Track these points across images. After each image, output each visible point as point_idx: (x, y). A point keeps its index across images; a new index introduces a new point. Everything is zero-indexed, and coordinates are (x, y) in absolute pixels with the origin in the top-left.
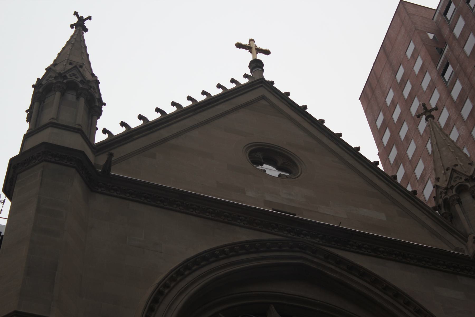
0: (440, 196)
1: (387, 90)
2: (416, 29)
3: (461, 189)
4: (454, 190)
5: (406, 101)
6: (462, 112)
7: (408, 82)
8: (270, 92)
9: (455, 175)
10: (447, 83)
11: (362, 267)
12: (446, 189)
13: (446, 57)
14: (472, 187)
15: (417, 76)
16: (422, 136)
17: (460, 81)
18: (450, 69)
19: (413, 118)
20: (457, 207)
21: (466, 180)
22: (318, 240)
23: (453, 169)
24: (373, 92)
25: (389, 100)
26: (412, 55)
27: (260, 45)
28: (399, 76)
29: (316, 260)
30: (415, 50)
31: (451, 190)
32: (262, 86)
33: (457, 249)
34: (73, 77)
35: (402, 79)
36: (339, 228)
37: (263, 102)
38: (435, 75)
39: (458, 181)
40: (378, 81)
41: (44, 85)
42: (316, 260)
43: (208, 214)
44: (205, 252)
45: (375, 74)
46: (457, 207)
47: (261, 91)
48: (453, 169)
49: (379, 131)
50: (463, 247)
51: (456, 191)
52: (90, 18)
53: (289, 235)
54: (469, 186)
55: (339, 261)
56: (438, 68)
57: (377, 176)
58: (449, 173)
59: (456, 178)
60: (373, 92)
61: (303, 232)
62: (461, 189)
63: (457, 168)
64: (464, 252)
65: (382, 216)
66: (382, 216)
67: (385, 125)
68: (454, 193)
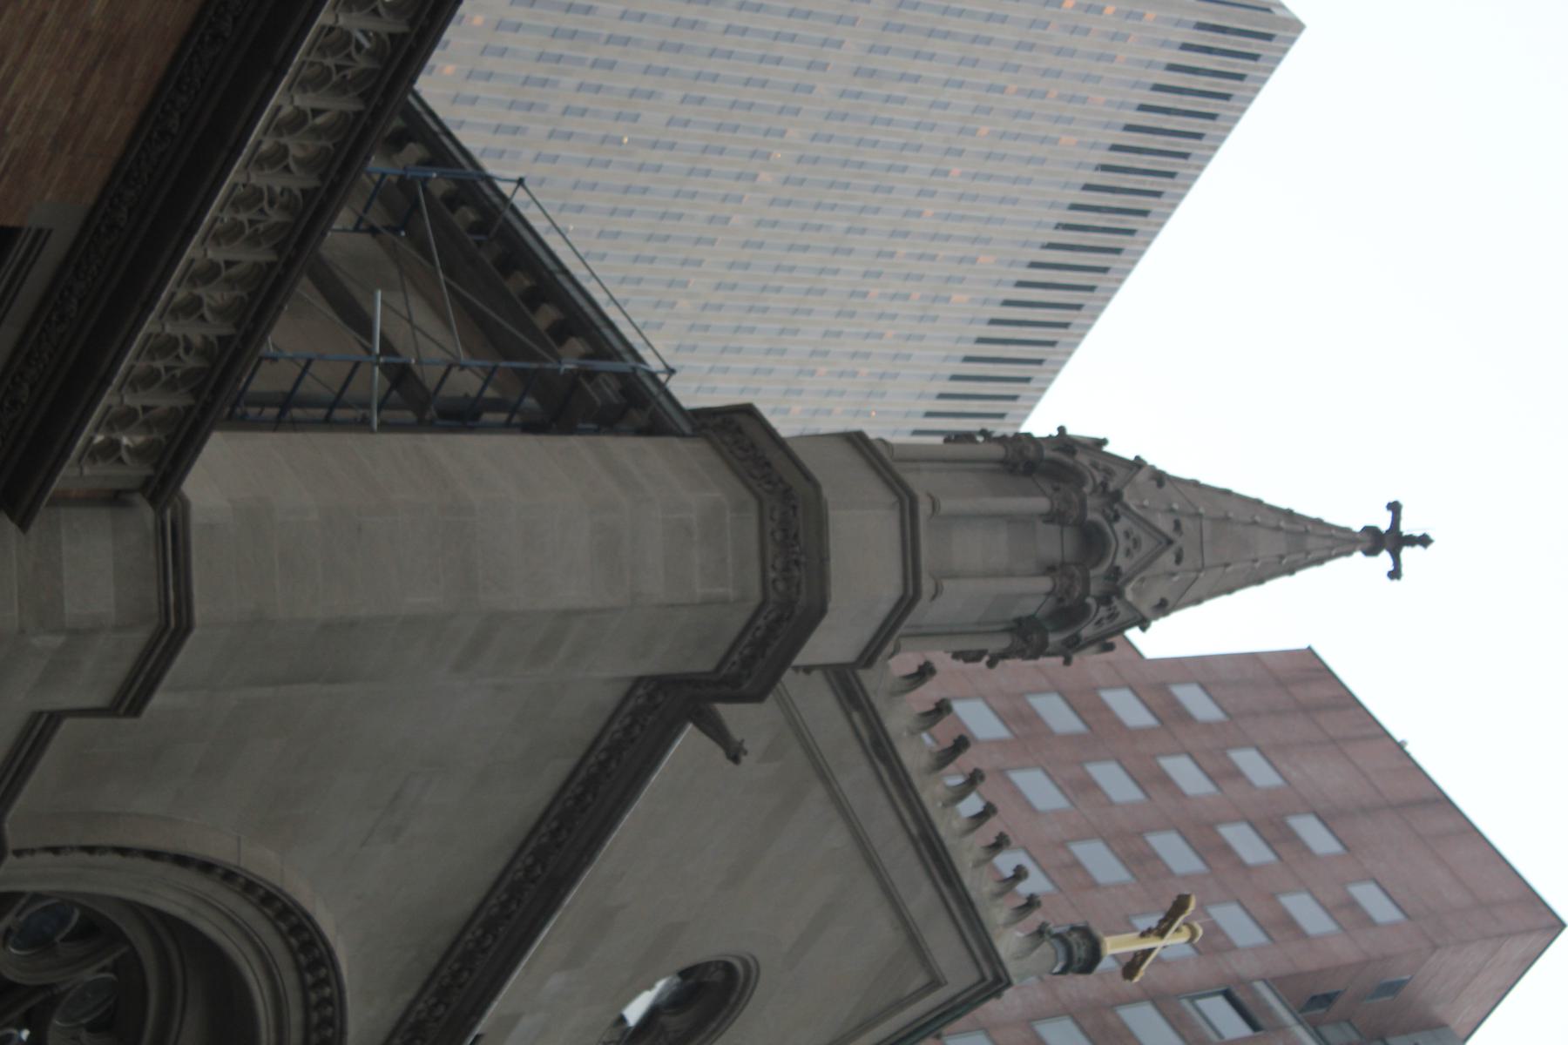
2: (1435, 947)
5: (1211, 826)
6: (1067, 1025)
10: (1192, 999)
13: (1281, 1028)
15: (1272, 897)
16: (1063, 844)
18: (1234, 1026)
19: (1140, 834)
25: (1248, 761)
26: (1352, 904)
28: (1311, 831)
30: (1367, 920)
35: (1292, 837)
38: (1244, 967)
40: (1333, 741)
41: (1112, 527)
49: (1162, 687)
52: (1395, 574)
56: (1260, 986)
67: (1172, 715)
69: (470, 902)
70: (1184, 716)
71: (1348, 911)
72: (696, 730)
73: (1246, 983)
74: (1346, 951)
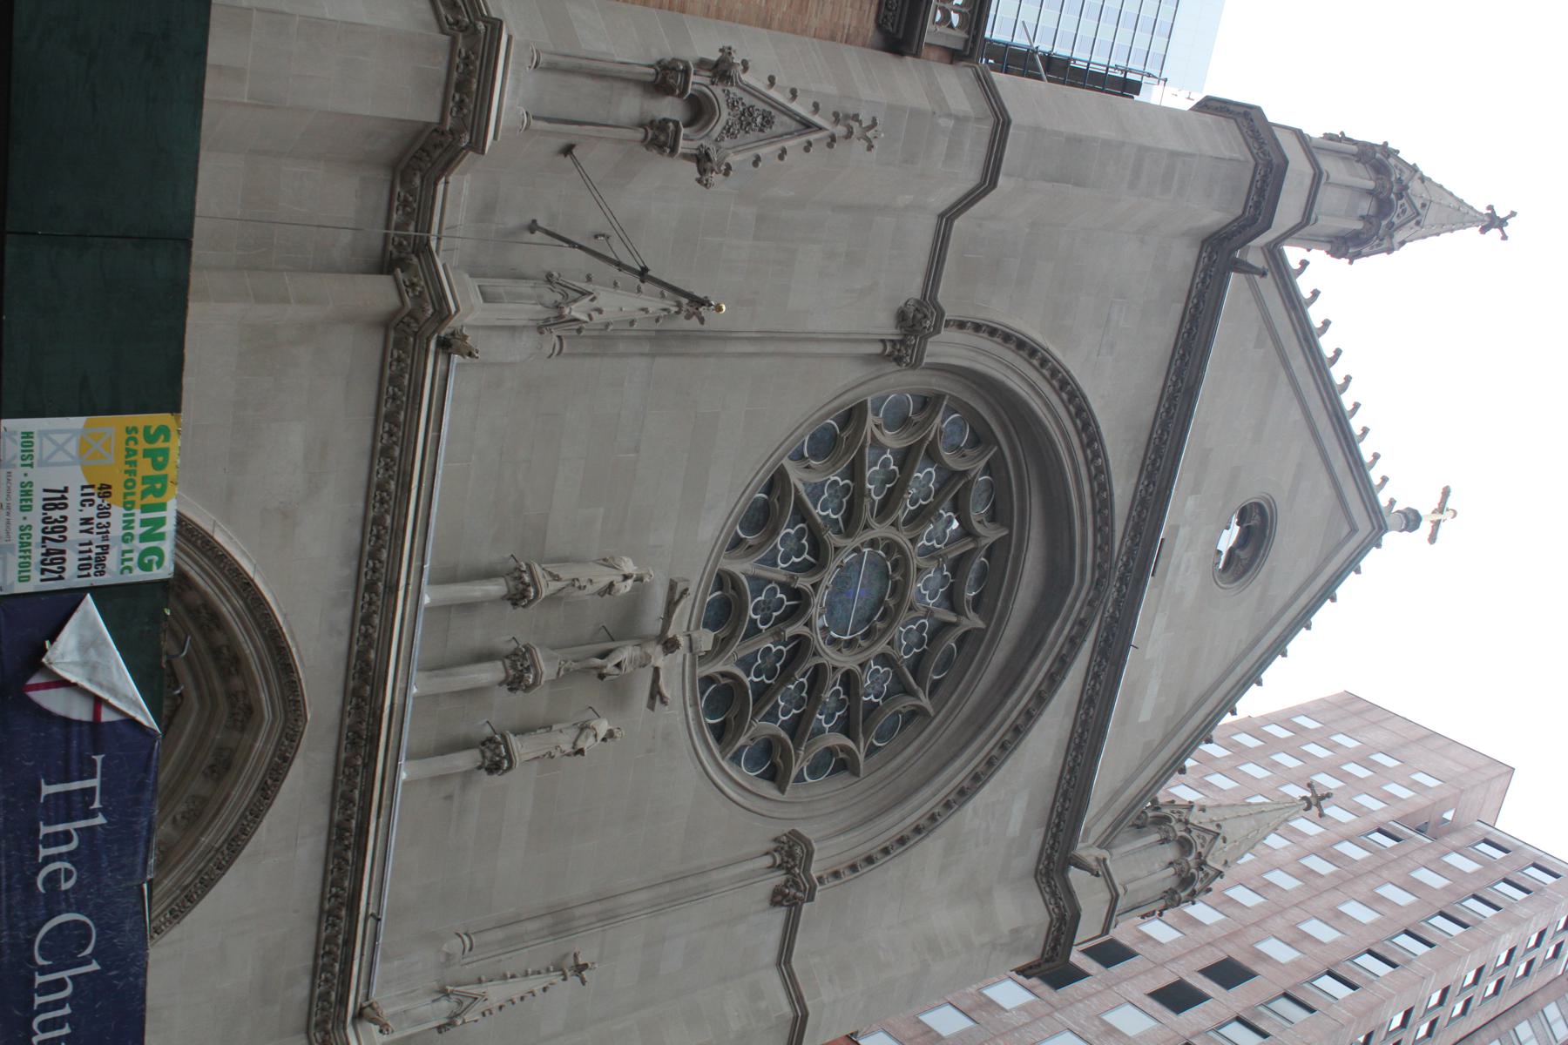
0: (1175, 810)
1: (1358, 738)
3: (1185, 845)
4: (1184, 834)
5: (1338, 767)
7: (1370, 773)
8: (1363, 542)
9: (1208, 837)
11: (1064, 678)
12: (1187, 822)
14: (1187, 862)
15: (1379, 788)
16: (1276, 789)
17: (1369, 858)
19: (1308, 777)
20: (1156, 837)
21: (1200, 854)
22: (1111, 610)
23: (1218, 834)
24: (1358, 714)
25: (1340, 739)
26: (1416, 783)
28: (1380, 758)
29: (1078, 605)
31: (1183, 828)
32: (1374, 528)
33: (1087, 831)
35: (1376, 763)
36: (1129, 645)
37: (1346, 530)
39: (1199, 842)
40: (1374, 723)
42: (1078, 605)
43: (1159, 432)
44: (1097, 427)
45: (1388, 719)
46: (1156, 837)
47: (1364, 526)
48: (1218, 834)
49: (1289, 720)
50: (1091, 841)
51: (1181, 837)
53: (1120, 564)
54: (1189, 859)
55: (1074, 643)
56: (1392, 823)
57: (1212, 712)
58: (1213, 828)
59: (1204, 839)
60: (1358, 714)
61: (1124, 587)
62: (1185, 845)
63: (1219, 841)
64: (1083, 841)
65: (1145, 715)
66: (1145, 715)
67: (1299, 730)
68: (1179, 834)
69: (1152, 409)
70: (1305, 729)
71: (1413, 785)
72: (1237, 274)
73: (1385, 823)
74: (1422, 801)
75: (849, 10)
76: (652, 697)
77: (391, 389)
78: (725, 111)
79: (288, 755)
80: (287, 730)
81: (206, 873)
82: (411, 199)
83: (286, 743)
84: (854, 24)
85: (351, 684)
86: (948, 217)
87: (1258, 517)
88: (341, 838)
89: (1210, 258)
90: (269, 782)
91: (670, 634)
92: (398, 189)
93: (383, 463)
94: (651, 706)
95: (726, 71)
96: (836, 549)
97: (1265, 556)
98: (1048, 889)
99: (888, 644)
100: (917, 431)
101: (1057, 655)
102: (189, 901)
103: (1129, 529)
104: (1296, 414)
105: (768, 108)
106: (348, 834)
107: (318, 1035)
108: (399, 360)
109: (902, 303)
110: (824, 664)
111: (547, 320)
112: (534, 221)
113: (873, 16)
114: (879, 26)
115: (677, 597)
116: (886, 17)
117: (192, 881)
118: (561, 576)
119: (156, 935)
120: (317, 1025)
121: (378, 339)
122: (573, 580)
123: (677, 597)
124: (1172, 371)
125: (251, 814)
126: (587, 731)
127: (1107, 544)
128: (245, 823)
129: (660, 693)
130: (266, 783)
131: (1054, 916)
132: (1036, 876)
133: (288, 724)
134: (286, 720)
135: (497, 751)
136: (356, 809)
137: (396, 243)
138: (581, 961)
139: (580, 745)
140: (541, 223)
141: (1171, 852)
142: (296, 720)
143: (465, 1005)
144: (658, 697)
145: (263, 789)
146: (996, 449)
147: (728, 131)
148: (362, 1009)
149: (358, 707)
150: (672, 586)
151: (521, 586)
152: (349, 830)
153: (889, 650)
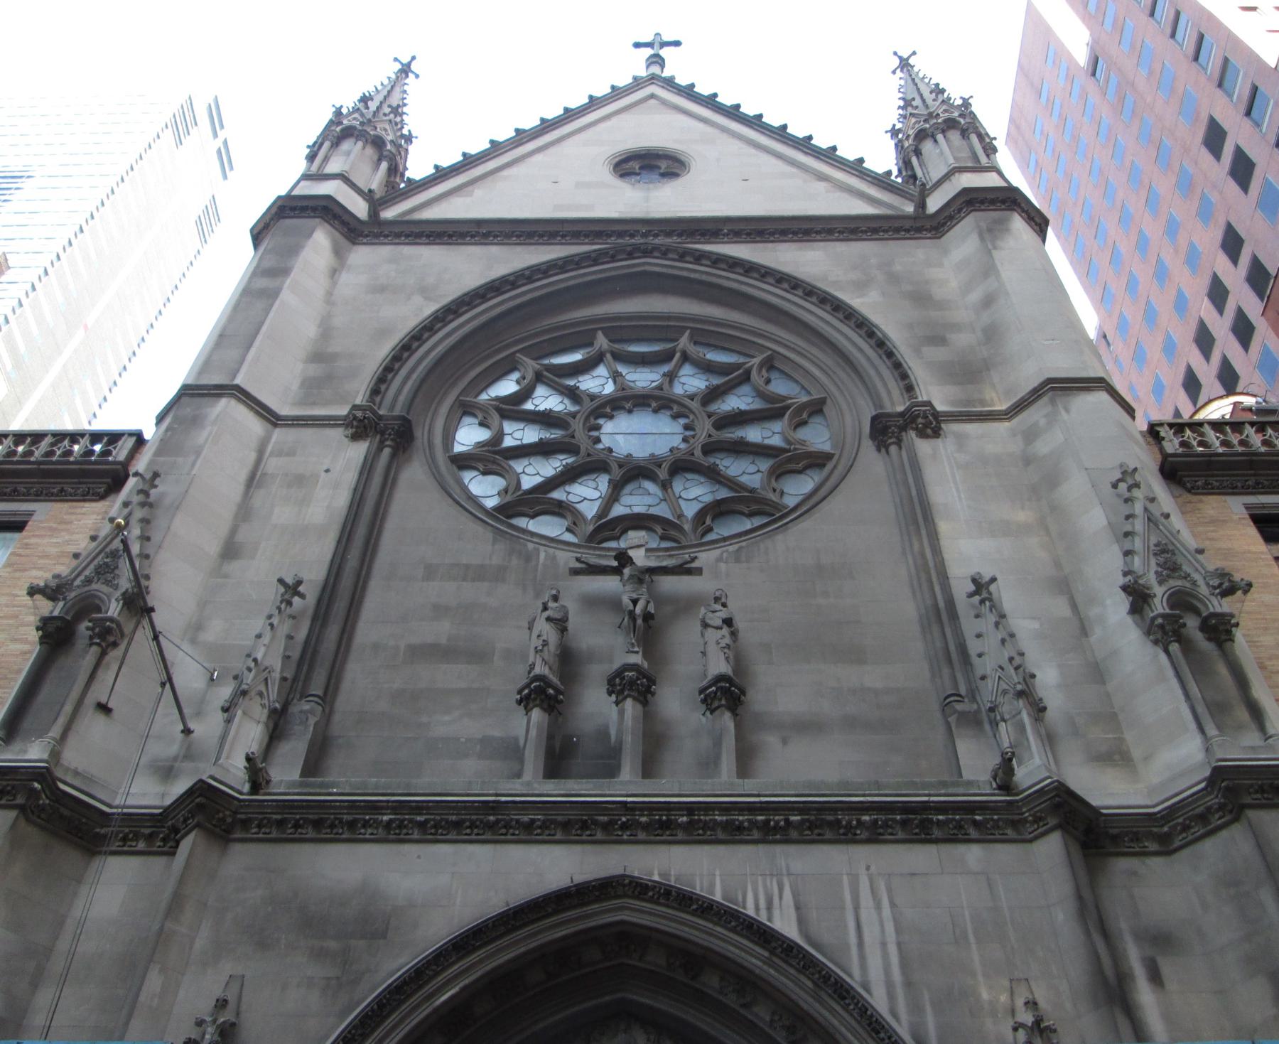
8: (663, 87)
27: (666, 38)
32: (653, 83)
34: (384, 133)
37: (652, 101)
55: (699, 257)
75: (82, 522)
76: (689, 572)
77: (289, 831)
78: (94, 586)
79: (662, 891)
80: (636, 893)
81: (798, 964)
82: (121, 835)
83: (650, 894)
84: (95, 517)
85: (599, 835)
86: (271, 418)
87: (631, 164)
88: (776, 829)
89: (367, 236)
90: (694, 907)
91: (615, 564)
92: (114, 848)
93: (362, 831)
94: (699, 571)
95: (53, 590)
96: (620, 466)
97: (663, 149)
98: (949, 223)
99: (692, 400)
100: (470, 406)
101: (695, 264)
102: (829, 979)
103: (601, 241)
104: (538, 158)
105: (103, 554)
106: (772, 823)
107: (1030, 830)
108: (259, 826)
109: (346, 440)
110: (702, 446)
111: (263, 706)
112: (183, 732)
113: (94, 504)
114: (102, 497)
115: (583, 566)
116: (93, 494)
117: (809, 978)
118: (530, 663)
119: (869, 1013)
120: (1019, 833)
121: (237, 848)
122: (537, 652)
123: (583, 566)
124: (462, 241)
125: (730, 922)
126: (707, 617)
127: (607, 253)
128: (741, 927)
129: (681, 565)
130: (696, 910)
131: (969, 209)
132: (940, 238)
133: (630, 893)
134: (625, 896)
135: (713, 695)
136: (741, 818)
137: (161, 844)
138: (972, 588)
139: (719, 622)
140: (181, 727)
141: (927, 146)
142: (624, 886)
143: (1005, 687)
144: (686, 566)
145: (703, 912)
146: (518, 355)
147: (110, 581)
148: (1000, 788)
149: (624, 827)
150: (575, 572)
151: (533, 696)
152: (768, 821)
153: (697, 399)
